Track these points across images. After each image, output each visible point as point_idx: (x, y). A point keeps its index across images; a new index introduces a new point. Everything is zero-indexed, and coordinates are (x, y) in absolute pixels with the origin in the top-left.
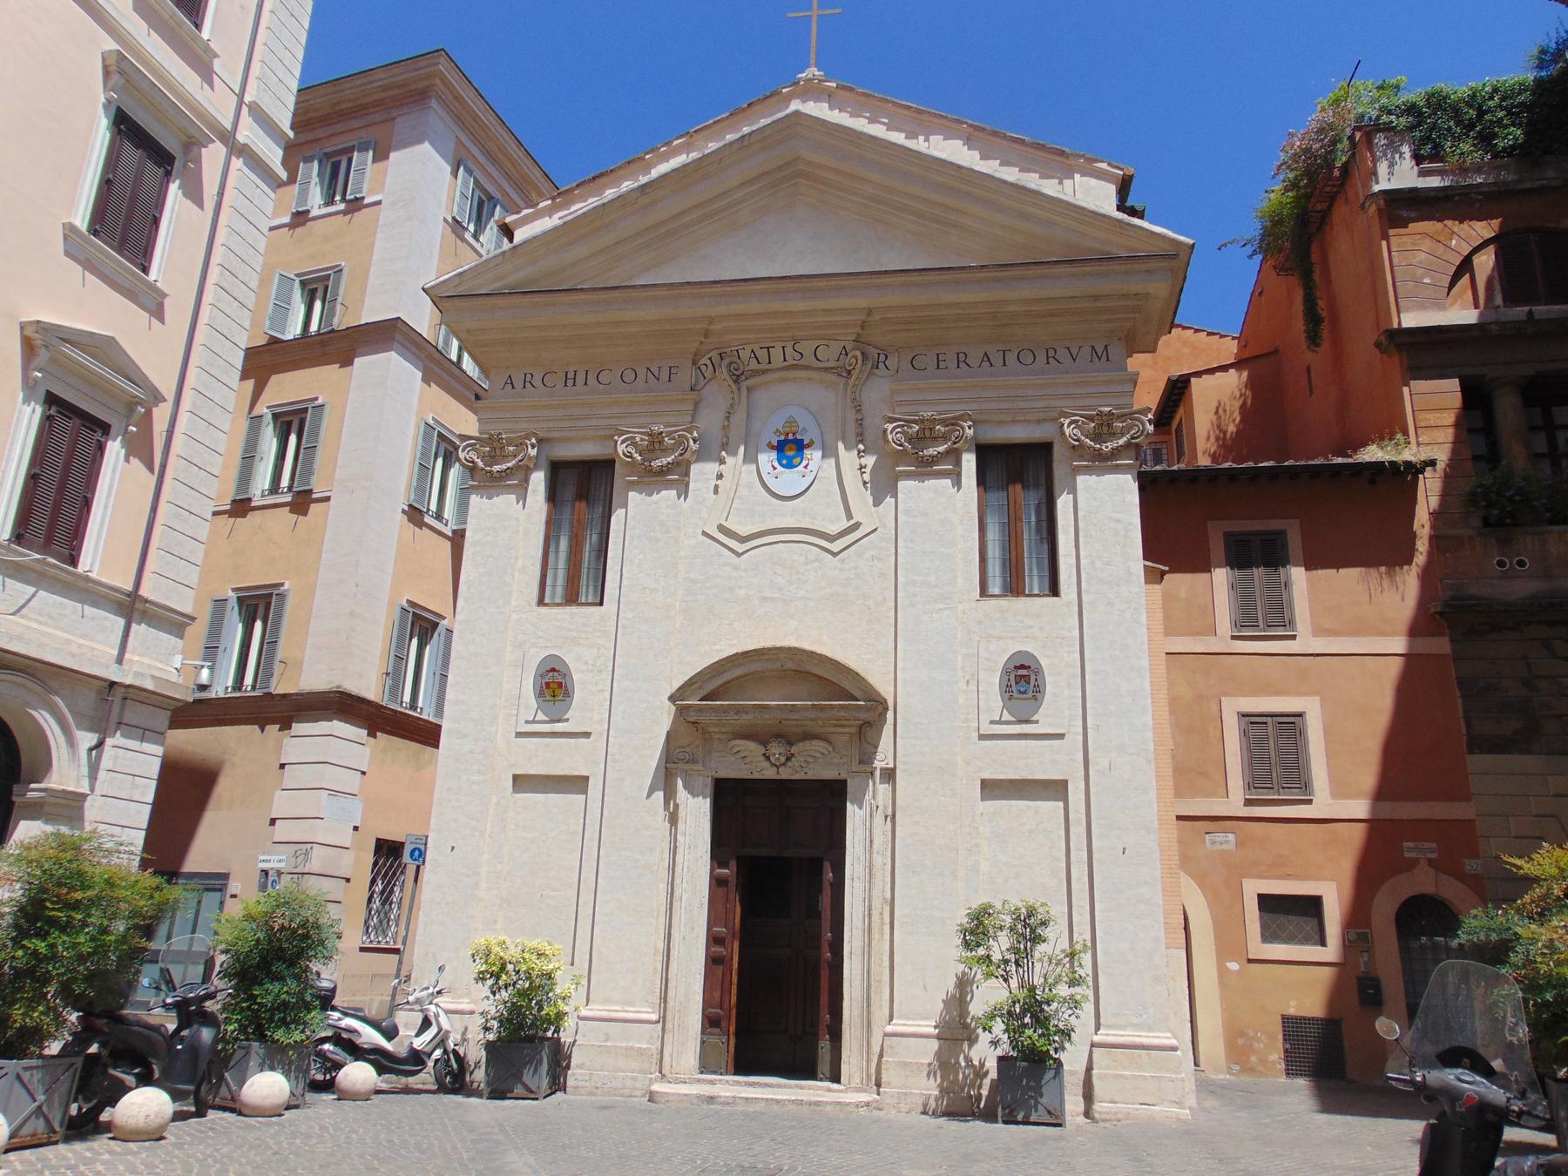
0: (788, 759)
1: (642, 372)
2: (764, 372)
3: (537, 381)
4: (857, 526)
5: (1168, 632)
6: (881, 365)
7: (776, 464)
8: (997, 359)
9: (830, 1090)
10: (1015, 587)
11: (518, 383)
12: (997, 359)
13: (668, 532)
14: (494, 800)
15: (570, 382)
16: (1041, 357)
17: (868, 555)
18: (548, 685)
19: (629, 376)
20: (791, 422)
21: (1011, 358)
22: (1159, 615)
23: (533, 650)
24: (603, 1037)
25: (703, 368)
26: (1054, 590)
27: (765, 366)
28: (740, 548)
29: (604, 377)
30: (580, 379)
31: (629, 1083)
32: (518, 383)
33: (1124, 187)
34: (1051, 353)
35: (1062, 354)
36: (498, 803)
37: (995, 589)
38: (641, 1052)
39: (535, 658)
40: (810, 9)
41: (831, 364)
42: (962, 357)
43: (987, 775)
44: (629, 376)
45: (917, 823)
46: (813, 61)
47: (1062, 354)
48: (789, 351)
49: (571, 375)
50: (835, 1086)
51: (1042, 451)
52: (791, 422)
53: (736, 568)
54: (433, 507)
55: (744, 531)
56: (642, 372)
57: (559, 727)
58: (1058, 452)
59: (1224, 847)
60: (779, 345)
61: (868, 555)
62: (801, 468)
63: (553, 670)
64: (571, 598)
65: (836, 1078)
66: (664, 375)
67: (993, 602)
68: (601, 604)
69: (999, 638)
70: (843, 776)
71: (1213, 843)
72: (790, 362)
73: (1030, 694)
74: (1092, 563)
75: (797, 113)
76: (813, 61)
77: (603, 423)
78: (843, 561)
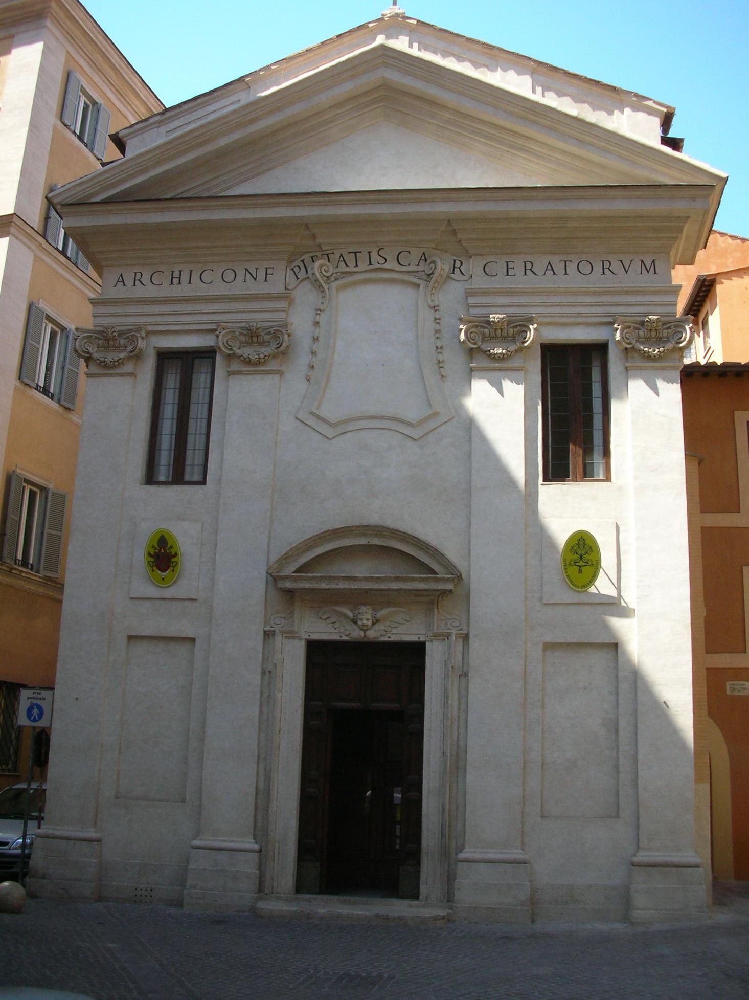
0: (374, 624)
1: (241, 273)
2: (351, 273)
3: (146, 279)
4: (436, 414)
5: (704, 510)
6: (457, 270)
8: (559, 268)
9: (410, 906)
12: (559, 268)
15: (175, 281)
16: (598, 268)
19: (229, 276)
21: (572, 268)
22: (697, 499)
25: (296, 269)
26: (608, 479)
27: (352, 268)
28: (329, 432)
29: (207, 277)
30: (185, 278)
32: (129, 281)
33: (667, 120)
34: (607, 265)
35: (616, 266)
41: (411, 268)
42: (529, 266)
43: (548, 639)
44: (229, 276)
47: (616, 266)
48: (374, 255)
49: (176, 274)
51: (601, 349)
54: (42, 384)
56: (241, 273)
57: (168, 593)
58: (614, 355)
59: (741, 694)
60: (365, 250)
64: (178, 478)
65: (415, 895)
66: (261, 276)
68: (203, 482)
70: (422, 639)
71: (733, 689)
72: (376, 266)
75: (383, 47)
77: (206, 318)
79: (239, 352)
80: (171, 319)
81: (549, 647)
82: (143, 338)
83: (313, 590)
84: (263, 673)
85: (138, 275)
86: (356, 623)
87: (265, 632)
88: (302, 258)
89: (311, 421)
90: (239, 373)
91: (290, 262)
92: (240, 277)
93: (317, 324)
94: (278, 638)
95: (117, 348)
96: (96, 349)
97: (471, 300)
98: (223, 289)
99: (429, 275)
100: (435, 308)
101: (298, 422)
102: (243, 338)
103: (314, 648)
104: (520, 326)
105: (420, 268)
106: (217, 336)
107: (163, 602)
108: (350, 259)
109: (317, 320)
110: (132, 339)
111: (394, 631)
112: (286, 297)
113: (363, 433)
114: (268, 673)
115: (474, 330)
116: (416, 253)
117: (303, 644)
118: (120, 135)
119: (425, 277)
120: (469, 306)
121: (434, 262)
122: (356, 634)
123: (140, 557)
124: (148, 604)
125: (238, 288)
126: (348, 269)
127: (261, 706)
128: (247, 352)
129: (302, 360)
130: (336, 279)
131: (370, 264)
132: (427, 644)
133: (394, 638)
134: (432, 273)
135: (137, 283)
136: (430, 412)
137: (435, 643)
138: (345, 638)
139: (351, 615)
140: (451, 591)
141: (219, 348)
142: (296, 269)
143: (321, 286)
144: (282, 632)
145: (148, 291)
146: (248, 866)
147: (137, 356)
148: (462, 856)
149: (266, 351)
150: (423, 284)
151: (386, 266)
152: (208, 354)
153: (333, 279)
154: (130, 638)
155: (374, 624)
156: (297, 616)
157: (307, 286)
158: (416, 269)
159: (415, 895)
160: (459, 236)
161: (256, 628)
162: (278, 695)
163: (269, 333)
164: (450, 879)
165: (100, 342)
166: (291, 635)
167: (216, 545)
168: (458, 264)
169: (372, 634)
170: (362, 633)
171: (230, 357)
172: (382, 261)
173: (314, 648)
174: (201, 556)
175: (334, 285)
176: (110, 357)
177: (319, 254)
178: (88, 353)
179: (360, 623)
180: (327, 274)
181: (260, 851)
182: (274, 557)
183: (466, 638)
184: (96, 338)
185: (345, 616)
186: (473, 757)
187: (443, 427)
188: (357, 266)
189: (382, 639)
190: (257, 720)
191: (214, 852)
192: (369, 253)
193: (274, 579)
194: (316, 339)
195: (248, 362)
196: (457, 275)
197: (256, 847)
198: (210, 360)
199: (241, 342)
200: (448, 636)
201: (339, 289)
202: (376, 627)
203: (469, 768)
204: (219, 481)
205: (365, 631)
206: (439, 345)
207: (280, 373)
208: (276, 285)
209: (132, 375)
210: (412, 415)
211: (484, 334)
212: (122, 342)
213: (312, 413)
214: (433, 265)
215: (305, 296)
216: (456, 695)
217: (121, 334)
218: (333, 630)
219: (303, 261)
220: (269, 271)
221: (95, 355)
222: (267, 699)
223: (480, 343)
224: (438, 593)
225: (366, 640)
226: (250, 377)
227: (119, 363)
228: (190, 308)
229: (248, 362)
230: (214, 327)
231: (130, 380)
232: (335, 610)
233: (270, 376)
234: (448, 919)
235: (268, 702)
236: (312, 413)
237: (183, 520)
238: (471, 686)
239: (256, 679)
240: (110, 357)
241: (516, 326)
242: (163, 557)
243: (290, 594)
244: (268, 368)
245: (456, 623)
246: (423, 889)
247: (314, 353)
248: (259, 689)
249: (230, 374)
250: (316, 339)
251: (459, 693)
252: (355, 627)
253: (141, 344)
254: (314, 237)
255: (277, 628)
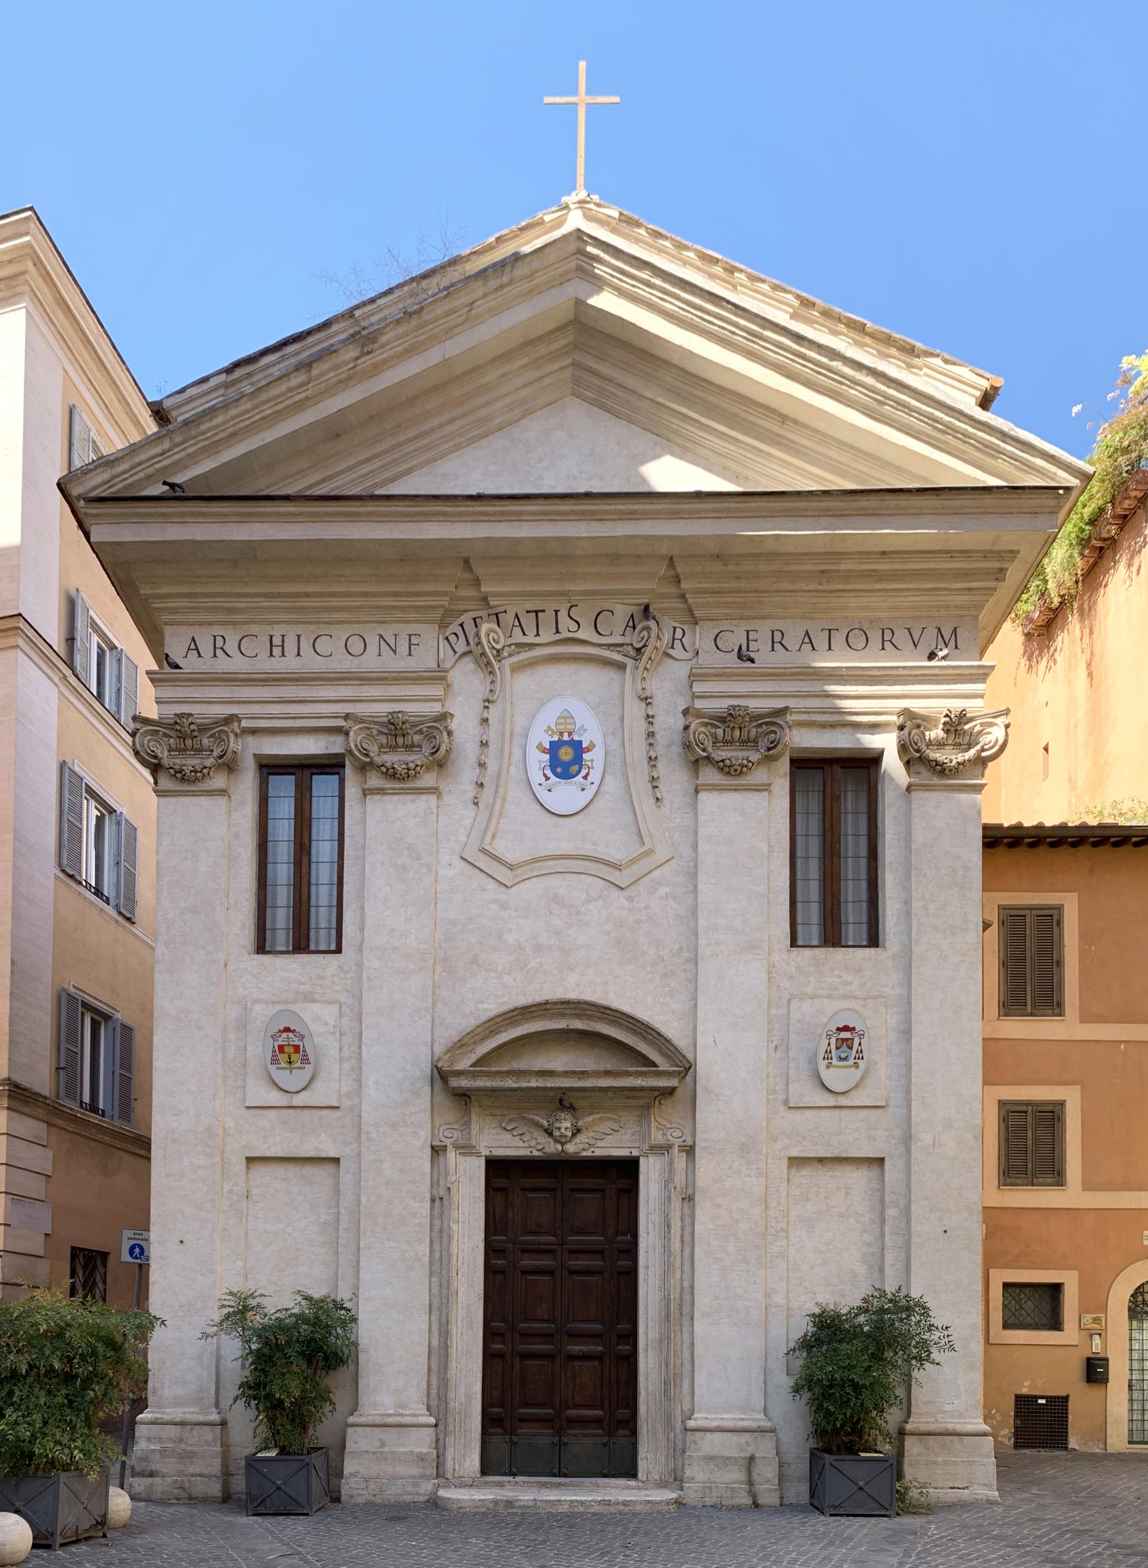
0: (574, 1135)
1: (373, 641)
2: (531, 646)
4: (650, 852)
6: (677, 643)
7: (549, 773)
10: (832, 937)
11: (206, 647)
13: (419, 857)
14: (226, 1188)
15: (277, 651)
17: (663, 891)
18: (281, 1048)
19: (356, 646)
20: (566, 717)
21: (838, 639)
23: (257, 1007)
24: (378, 1444)
25: (453, 638)
27: (531, 639)
29: (323, 645)
31: (410, 1488)
32: (206, 647)
36: (231, 1191)
37: (815, 933)
38: (422, 1458)
39: (261, 1013)
40: (575, 92)
44: (356, 646)
45: (719, 1206)
46: (581, 180)
49: (277, 641)
50: (632, 1483)
52: (566, 717)
53: (503, 906)
55: (512, 855)
56: (373, 641)
57: (298, 1100)
61: (663, 891)
62: (579, 778)
63: (287, 1030)
65: (631, 1472)
67: (807, 952)
69: (813, 997)
70: (635, 1153)
72: (565, 634)
73: (851, 1061)
74: (925, 908)
76: (581, 180)
78: (630, 899)
79: (378, 760)
80: (276, 709)
81: (796, 1162)
82: (236, 735)
83: (494, 1090)
84: (433, 1201)
85: (219, 639)
86: (550, 1134)
87: (432, 1147)
88: (459, 621)
89: (483, 862)
90: (381, 791)
91: (443, 625)
92: (372, 648)
93: (485, 721)
94: (451, 1154)
95: (199, 750)
96: (166, 753)
97: (698, 688)
98: (346, 664)
99: (638, 650)
100: (647, 700)
101: (464, 864)
102: (383, 739)
103: (496, 1168)
104: (766, 723)
105: (627, 640)
106: (347, 734)
107: (291, 1111)
108: (528, 622)
109: (486, 715)
110: (220, 738)
111: (599, 1144)
112: (438, 676)
113: (552, 878)
114: (439, 1200)
115: (702, 729)
116: (622, 612)
117: (483, 1161)
118: (167, 404)
119: (632, 653)
120: (694, 697)
121: (648, 628)
122: (552, 1148)
123: (259, 1049)
124: (271, 1114)
125: (371, 662)
126: (525, 640)
127: (431, 1243)
128: (390, 759)
129: (465, 773)
130: (510, 655)
131: (557, 632)
132: (642, 1161)
133: (599, 1153)
134: (645, 646)
135: (219, 652)
136: (642, 850)
137: (652, 1159)
138: (536, 1153)
139: (545, 1123)
140: (671, 1091)
141: (350, 752)
142: (453, 638)
143: (489, 663)
144: (456, 1147)
145: (237, 664)
146: (421, 1442)
147: (229, 765)
148: (691, 1424)
149: (414, 758)
150: (630, 663)
151: (579, 635)
152: (332, 765)
153: (505, 654)
154: (250, 1160)
155: (574, 1135)
156: (475, 1127)
157: (468, 665)
158: (619, 640)
159: (631, 1472)
160: (685, 585)
161: (421, 1141)
162: (454, 1227)
163: (421, 732)
164: (678, 1452)
165: (172, 741)
166: (466, 1149)
167: (361, 1033)
168: (679, 634)
169: (571, 1148)
170: (559, 1147)
171: (364, 768)
172: (574, 627)
173: (496, 1168)
174: (341, 1050)
175: (507, 663)
176: (190, 763)
177: (484, 614)
178: (155, 757)
179: (556, 1133)
180: (498, 647)
181: (436, 1425)
182: (439, 1050)
183: (690, 1151)
184: (165, 735)
185: (538, 1125)
186: (703, 1302)
187: (657, 873)
188: (538, 635)
189: (584, 1154)
190: (427, 1259)
191: (377, 1430)
192: (556, 612)
193: (441, 1076)
194: (484, 744)
195: (391, 774)
196: (677, 652)
197: (432, 1420)
198: (337, 777)
199: (381, 746)
200: (668, 1148)
201: (516, 669)
202: (580, 1138)
203: (697, 1315)
204: (360, 949)
205: (563, 1144)
206: (653, 755)
207: (435, 791)
208: (424, 659)
209: (223, 792)
210: (617, 856)
211: (715, 736)
212: (205, 741)
213: (484, 851)
214: (645, 633)
215: (467, 681)
216: (679, 1224)
217: (203, 729)
218: (521, 1144)
219: (461, 625)
220: (414, 640)
221: (166, 762)
222: (440, 1235)
223: (710, 749)
224: (656, 1093)
225: (564, 1157)
226: (396, 797)
227: (200, 774)
228: (302, 692)
229: (391, 774)
230: (341, 723)
231: (222, 801)
232: (525, 1118)
233: (424, 797)
234: (678, 1502)
235: (441, 1237)
236: (484, 851)
237: (314, 1001)
238: (698, 1212)
239: (424, 1208)
240: (190, 763)
241: (760, 725)
242: (290, 1049)
243: (463, 1097)
244: (419, 784)
245: (678, 1133)
246: (642, 1465)
247: (482, 765)
248: (426, 1222)
249: (366, 793)
250: (484, 744)
251: (682, 1221)
252: (550, 1140)
253: (234, 744)
254: (477, 583)
255: (448, 1142)
